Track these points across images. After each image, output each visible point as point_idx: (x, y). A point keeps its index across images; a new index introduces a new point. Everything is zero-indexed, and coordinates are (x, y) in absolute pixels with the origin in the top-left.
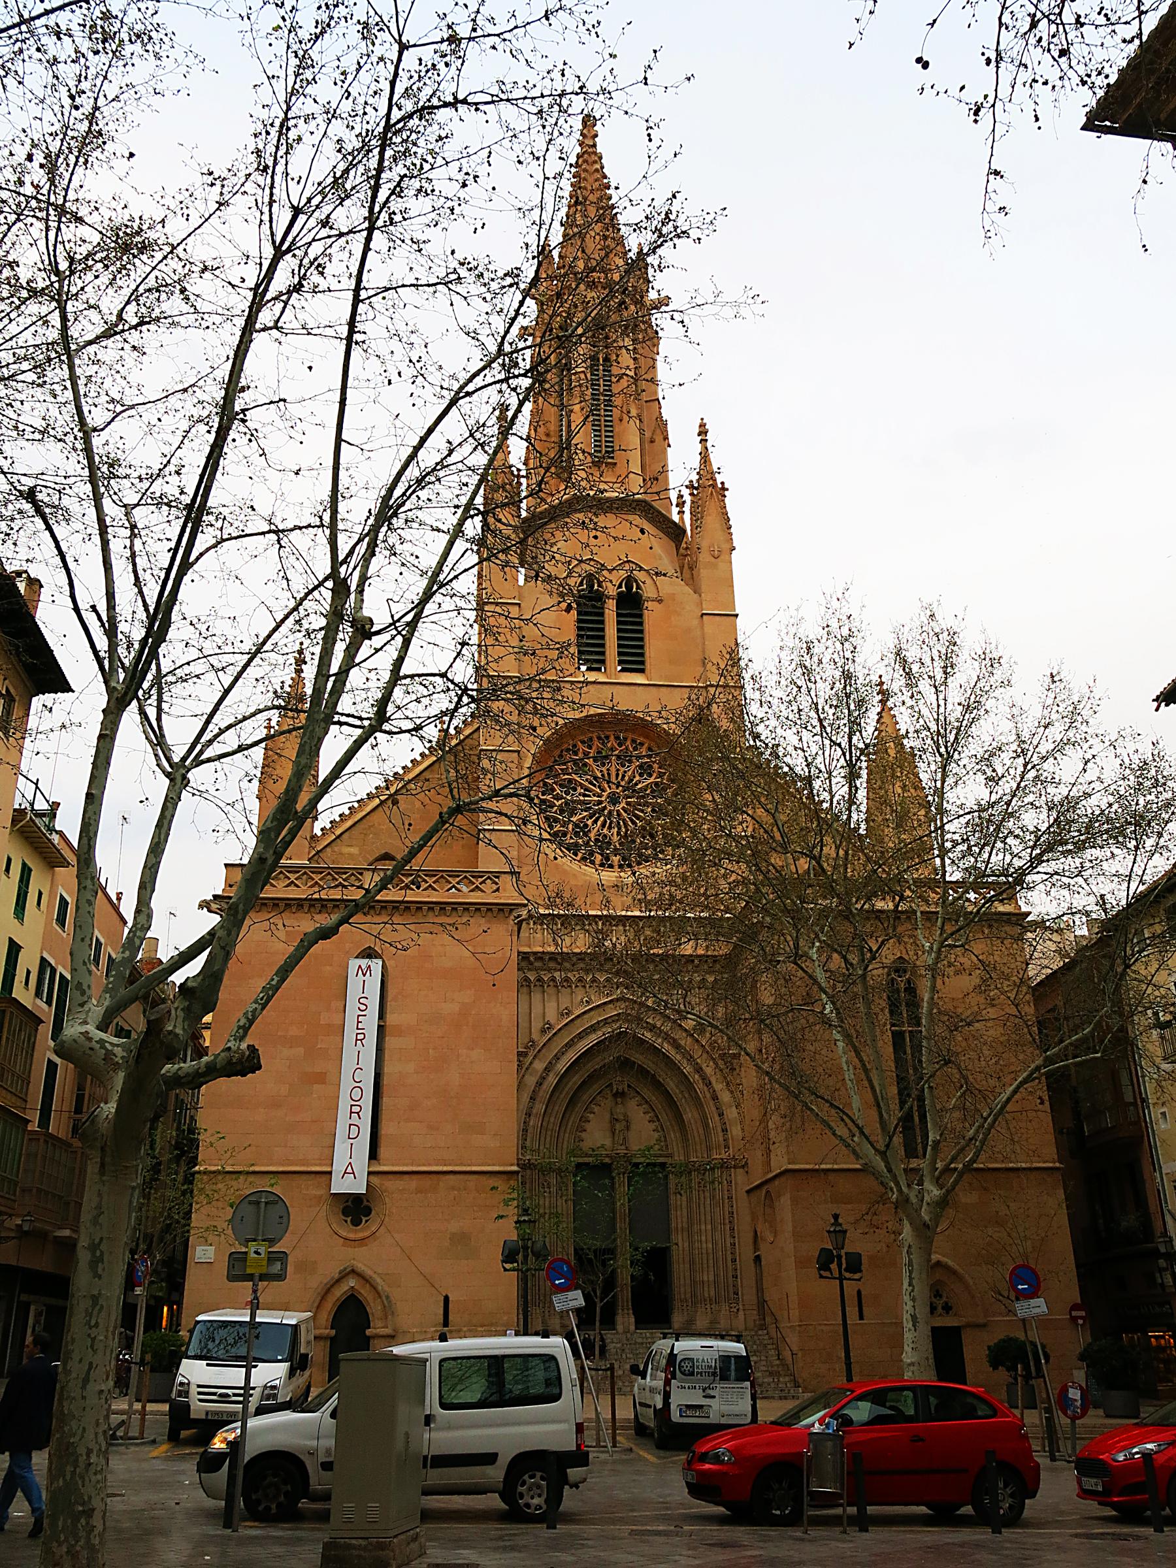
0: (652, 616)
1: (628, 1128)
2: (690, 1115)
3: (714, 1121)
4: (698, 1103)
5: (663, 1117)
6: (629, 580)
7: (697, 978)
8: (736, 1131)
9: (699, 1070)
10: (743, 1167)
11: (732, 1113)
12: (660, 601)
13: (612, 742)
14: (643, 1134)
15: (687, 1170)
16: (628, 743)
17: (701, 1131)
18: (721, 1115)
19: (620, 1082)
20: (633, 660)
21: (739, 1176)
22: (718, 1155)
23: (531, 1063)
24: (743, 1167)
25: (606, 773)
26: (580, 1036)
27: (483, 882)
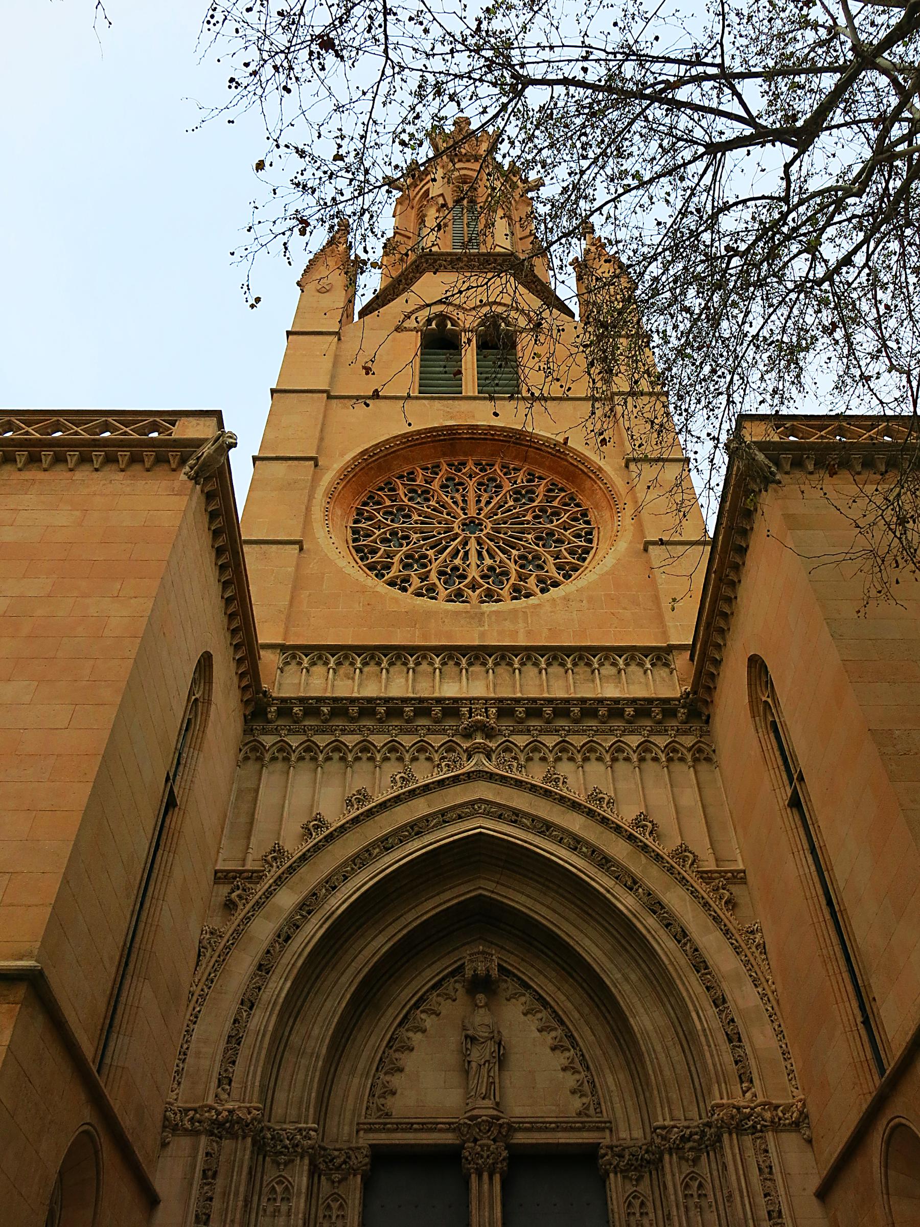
1: (501, 1060)
2: (646, 1019)
3: (706, 1018)
4: (660, 982)
5: (586, 1036)
7: (634, 741)
8: (761, 1039)
9: (655, 906)
10: (796, 1125)
11: (744, 997)
14: (540, 1085)
15: (645, 1163)
17: (677, 1055)
18: (719, 1002)
19: (481, 958)
22: (729, 1096)
23: (269, 894)
24: (796, 1125)
26: (386, 844)
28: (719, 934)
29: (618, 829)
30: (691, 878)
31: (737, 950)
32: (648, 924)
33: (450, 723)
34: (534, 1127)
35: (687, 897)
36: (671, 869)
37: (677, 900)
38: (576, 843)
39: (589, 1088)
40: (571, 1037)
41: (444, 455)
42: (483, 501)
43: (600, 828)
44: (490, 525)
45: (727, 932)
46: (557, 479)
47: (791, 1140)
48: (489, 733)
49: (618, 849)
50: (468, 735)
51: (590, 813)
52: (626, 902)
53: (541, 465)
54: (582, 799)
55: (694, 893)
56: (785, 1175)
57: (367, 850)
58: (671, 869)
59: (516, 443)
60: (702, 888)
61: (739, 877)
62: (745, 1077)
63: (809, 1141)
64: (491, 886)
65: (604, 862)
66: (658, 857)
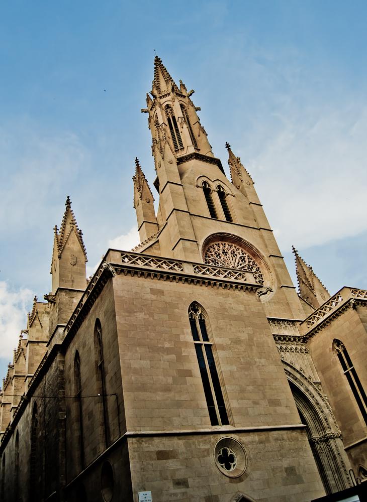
6: (219, 186)
9: (308, 390)
24: (339, 437)
30: (313, 384)
31: (323, 400)
32: (307, 394)
37: (310, 388)
41: (220, 241)
45: (321, 396)
47: (339, 439)
49: (298, 376)
53: (245, 249)
54: (289, 363)
55: (314, 387)
58: (308, 381)
62: (329, 428)
63: (342, 440)
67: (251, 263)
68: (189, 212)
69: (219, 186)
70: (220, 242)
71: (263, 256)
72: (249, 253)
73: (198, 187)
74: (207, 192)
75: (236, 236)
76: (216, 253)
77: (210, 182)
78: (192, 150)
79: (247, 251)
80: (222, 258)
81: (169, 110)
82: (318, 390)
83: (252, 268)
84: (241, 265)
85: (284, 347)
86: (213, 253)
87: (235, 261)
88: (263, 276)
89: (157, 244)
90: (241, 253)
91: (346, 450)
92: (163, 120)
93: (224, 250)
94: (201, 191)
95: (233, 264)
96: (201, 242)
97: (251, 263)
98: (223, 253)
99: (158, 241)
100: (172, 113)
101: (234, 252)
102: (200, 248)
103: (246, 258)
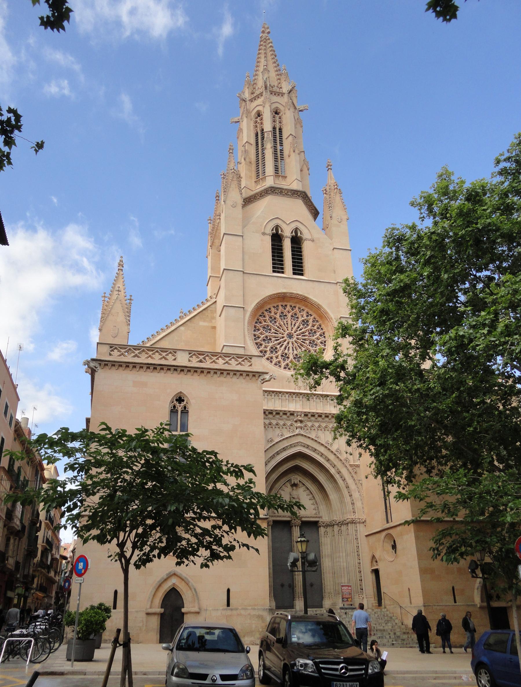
0: (307, 248)
3: (348, 499)
6: (296, 230)
9: (339, 473)
11: (356, 495)
12: (313, 241)
13: (288, 308)
15: (331, 525)
16: (297, 308)
19: (296, 478)
20: (298, 268)
21: (361, 528)
22: (350, 517)
25: (285, 323)
26: (278, 453)
27: (243, 361)
28: (352, 480)
29: (332, 452)
30: (348, 466)
31: (356, 484)
32: (337, 477)
33: (292, 417)
34: (306, 517)
35: (346, 470)
36: (343, 463)
37: (344, 471)
38: (322, 455)
39: (317, 509)
40: (314, 497)
41: (281, 302)
42: (293, 323)
43: (328, 451)
44: (296, 337)
46: (316, 317)
47: (362, 525)
48: (301, 421)
49: (331, 457)
50: (296, 422)
51: (326, 447)
52: (333, 471)
53: (311, 310)
54: (324, 443)
55: (348, 470)
56: (360, 532)
57: (274, 455)
58: (343, 463)
59: (303, 300)
60: (350, 469)
61: (358, 466)
62: (354, 512)
64: (299, 462)
65: (328, 460)
66: (341, 460)
67: (315, 328)
68: (243, 272)
69: (296, 230)
70: (280, 304)
71: (332, 318)
72: (316, 314)
73: (264, 234)
74: (277, 239)
75: (301, 295)
76: (271, 317)
77: (283, 226)
78: (270, 182)
79: (314, 312)
80: (277, 324)
81: (258, 120)
82: (353, 474)
83: (315, 332)
84: (301, 329)
85: (324, 425)
86: (267, 318)
87: (295, 325)
88: (327, 342)
89: (213, 306)
90: (305, 315)
91: (366, 536)
92: (248, 136)
93: (282, 313)
94: (269, 239)
95: (290, 329)
96: (250, 307)
97: (315, 328)
98: (280, 316)
99: (216, 302)
100: (262, 123)
101: (296, 314)
102: (248, 314)
103: (311, 322)
